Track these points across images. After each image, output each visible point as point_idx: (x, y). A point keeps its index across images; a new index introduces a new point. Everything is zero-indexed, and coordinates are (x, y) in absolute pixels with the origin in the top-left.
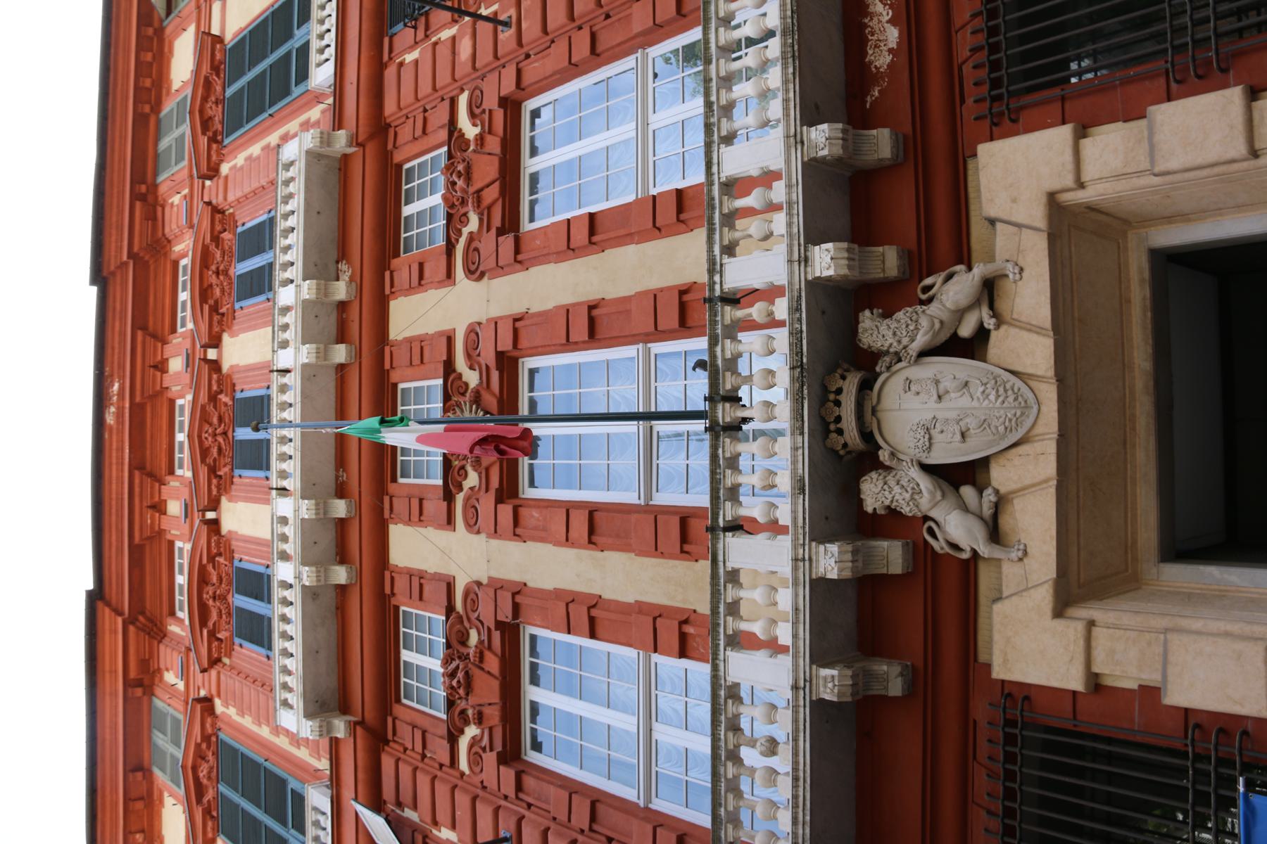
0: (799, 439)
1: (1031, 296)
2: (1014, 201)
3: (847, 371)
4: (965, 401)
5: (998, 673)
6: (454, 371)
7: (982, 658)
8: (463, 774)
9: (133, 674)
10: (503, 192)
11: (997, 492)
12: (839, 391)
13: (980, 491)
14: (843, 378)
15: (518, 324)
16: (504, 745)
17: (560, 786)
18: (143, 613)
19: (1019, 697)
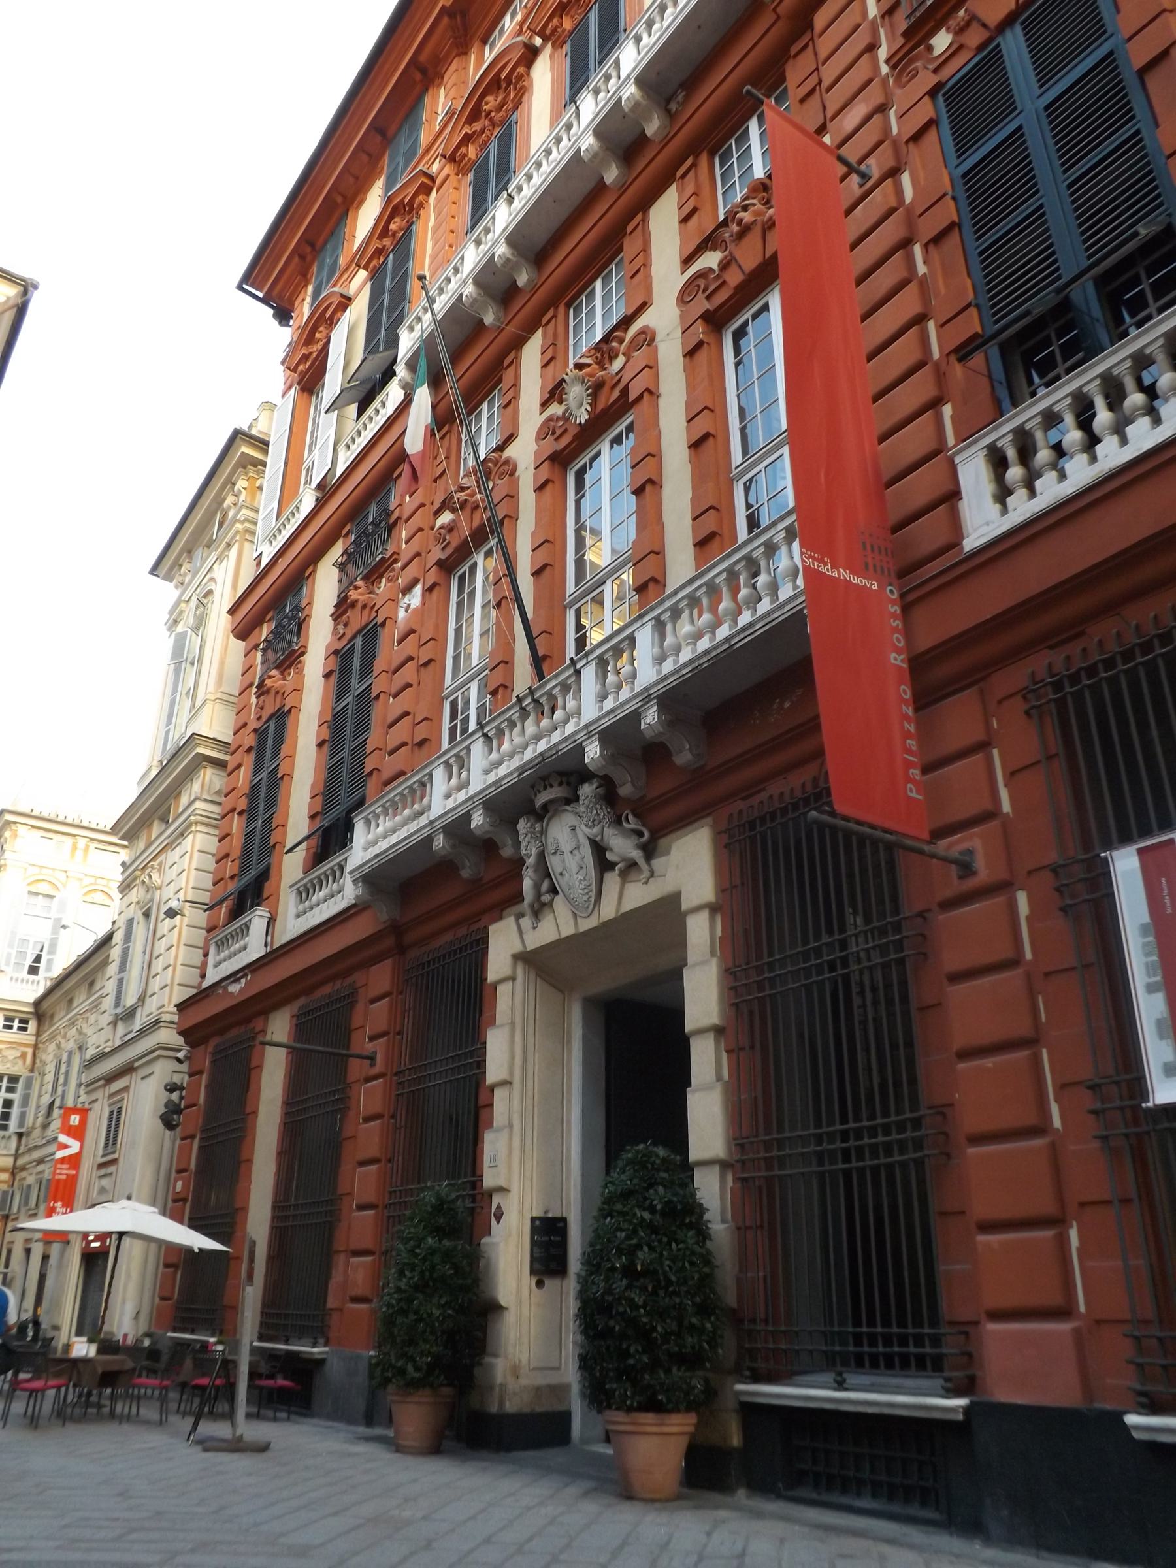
0: (515, 775)
1: (638, 895)
2: (677, 866)
3: (568, 784)
4: (574, 868)
5: (493, 929)
6: (626, 330)
7: (505, 913)
8: (432, 528)
9: (423, 58)
10: (740, 288)
11: (552, 901)
12: (551, 786)
13: (548, 892)
14: (560, 784)
15: (646, 395)
16: (447, 559)
17: (437, 626)
18: (464, 15)
19: (481, 945)
